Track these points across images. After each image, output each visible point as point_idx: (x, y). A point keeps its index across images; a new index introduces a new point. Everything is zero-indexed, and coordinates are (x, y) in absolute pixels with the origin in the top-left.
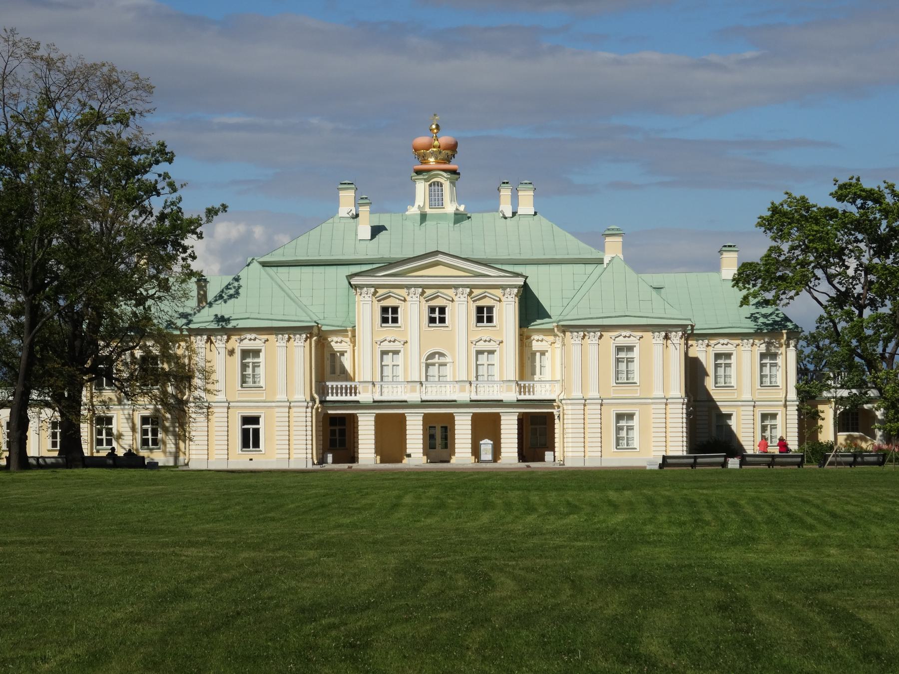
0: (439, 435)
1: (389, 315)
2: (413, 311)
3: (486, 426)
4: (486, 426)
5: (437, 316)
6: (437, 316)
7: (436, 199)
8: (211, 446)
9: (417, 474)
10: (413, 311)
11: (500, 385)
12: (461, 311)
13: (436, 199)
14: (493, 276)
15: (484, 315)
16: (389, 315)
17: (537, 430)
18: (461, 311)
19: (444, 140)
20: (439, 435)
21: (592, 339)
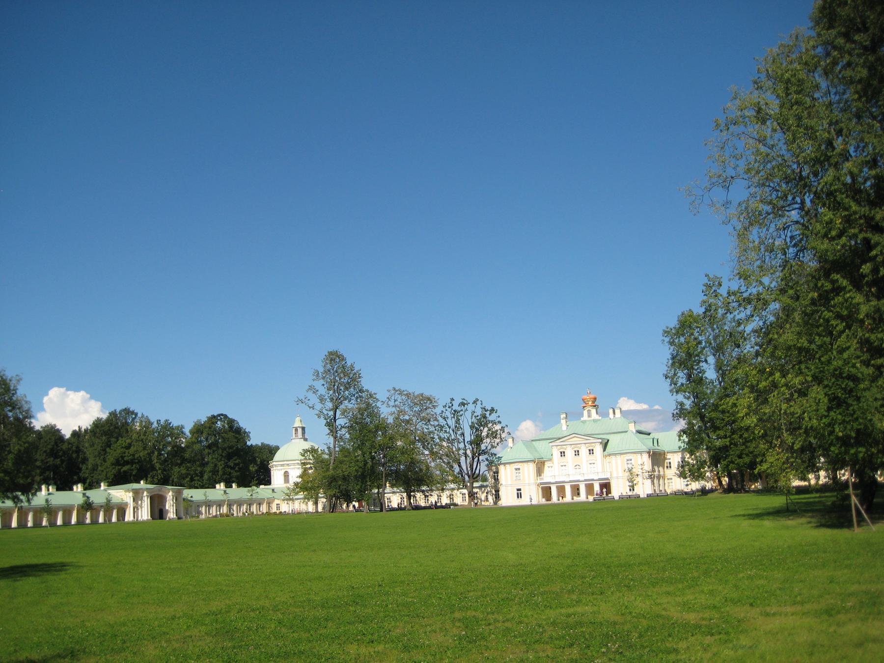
0: (576, 491)
1: (563, 454)
2: (570, 452)
5: (577, 453)
6: (577, 453)
7: (589, 416)
8: (508, 499)
9: (555, 505)
10: (570, 452)
12: (584, 451)
13: (589, 416)
14: (592, 440)
15: (591, 452)
16: (563, 454)
17: (606, 486)
18: (584, 451)
19: (592, 396)
20: (576, 491)
21: (618, 457)
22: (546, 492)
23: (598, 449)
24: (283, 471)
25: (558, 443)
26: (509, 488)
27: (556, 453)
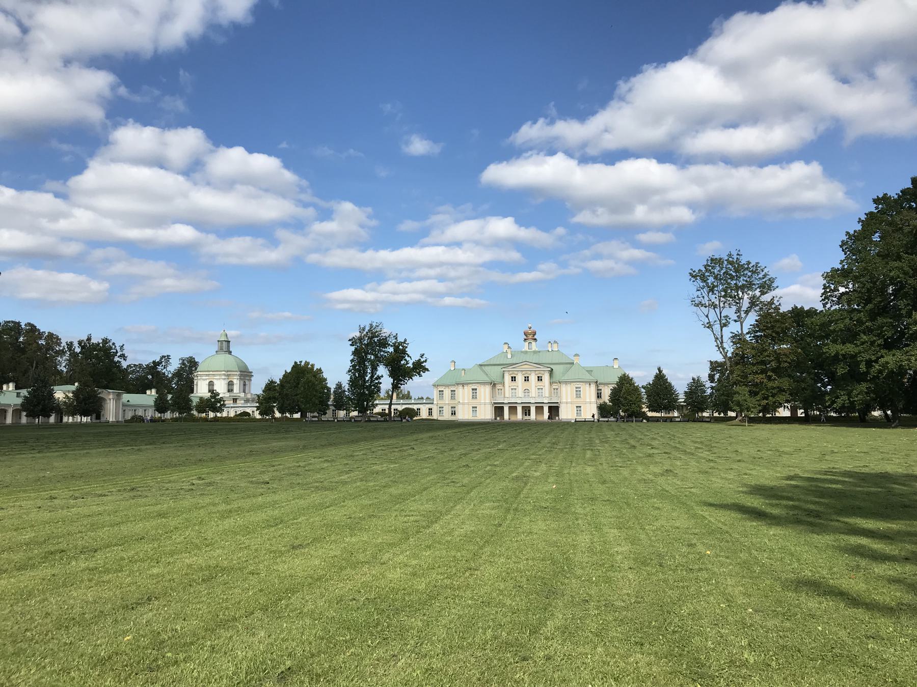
1: (513, 379)
2: (520, 378)
3: (539, 409)
4: (539, 409)
5: (527, 379)
6: (527, 379)
10: (520, 378)
11: (546, 397)
12: (533, 378)
14: (542, 368)
16: (513, 379)
17: (554, 410)
18: (533, 378)
20: (526, 411)
21: (569, 385)
22: (499, 410)
23: (546, 378)
24: (207, 382)
25: (510, 368)
26: (466, 406)
27: (507, 378)
